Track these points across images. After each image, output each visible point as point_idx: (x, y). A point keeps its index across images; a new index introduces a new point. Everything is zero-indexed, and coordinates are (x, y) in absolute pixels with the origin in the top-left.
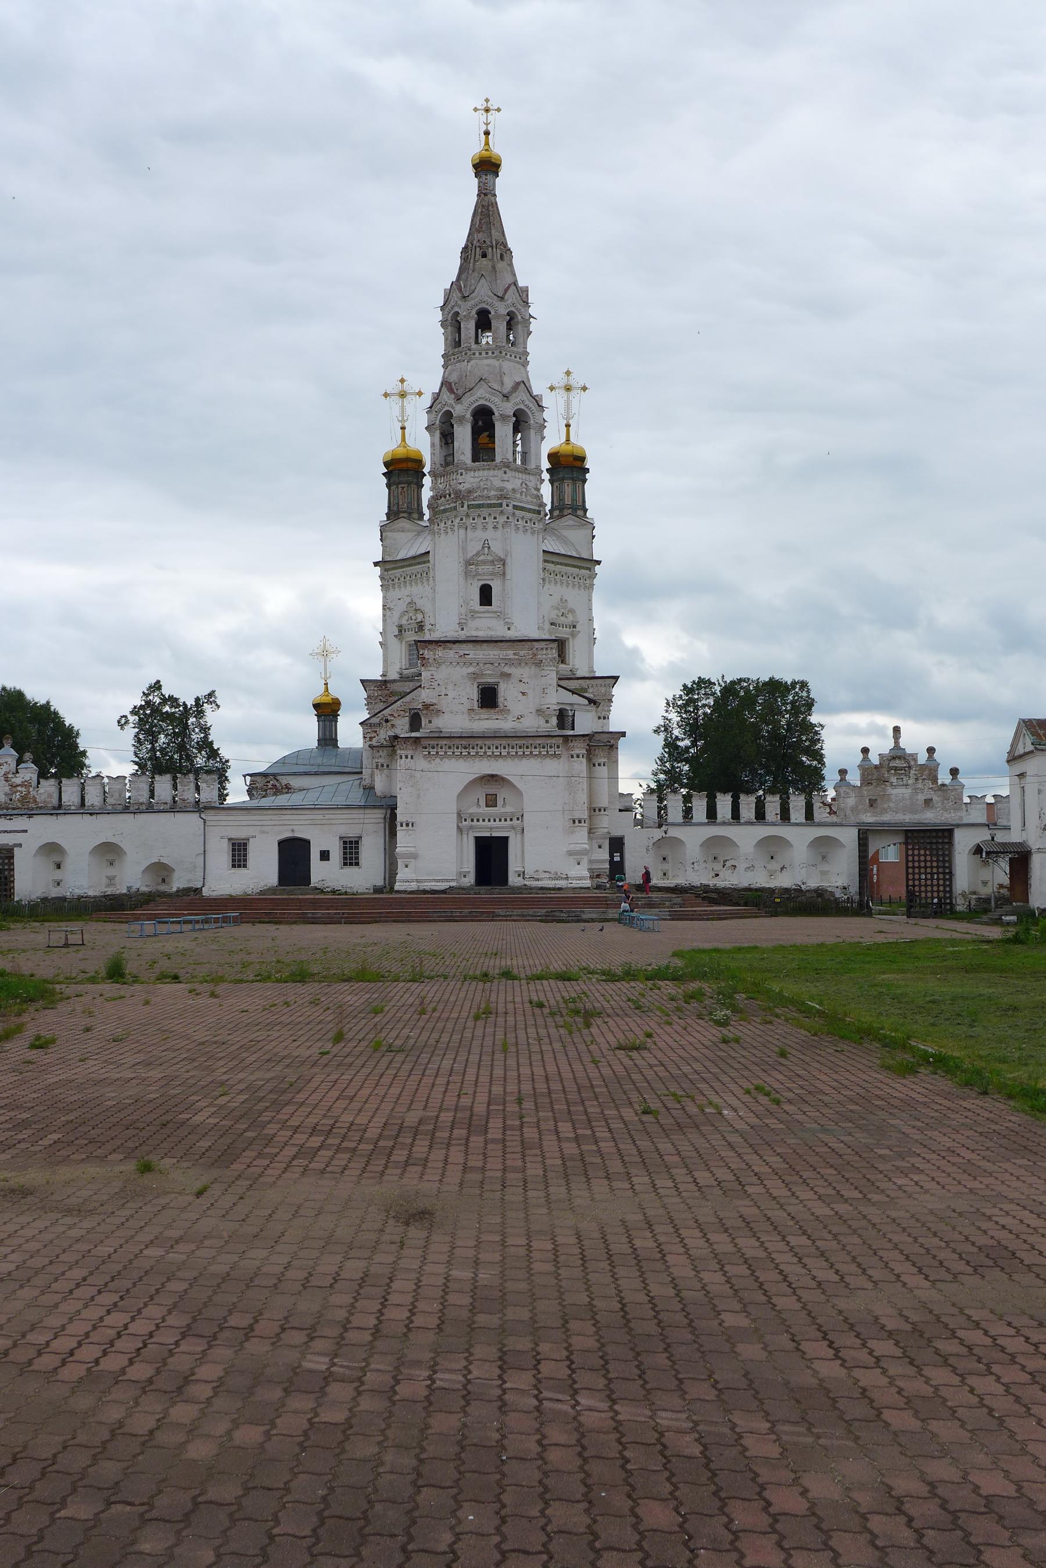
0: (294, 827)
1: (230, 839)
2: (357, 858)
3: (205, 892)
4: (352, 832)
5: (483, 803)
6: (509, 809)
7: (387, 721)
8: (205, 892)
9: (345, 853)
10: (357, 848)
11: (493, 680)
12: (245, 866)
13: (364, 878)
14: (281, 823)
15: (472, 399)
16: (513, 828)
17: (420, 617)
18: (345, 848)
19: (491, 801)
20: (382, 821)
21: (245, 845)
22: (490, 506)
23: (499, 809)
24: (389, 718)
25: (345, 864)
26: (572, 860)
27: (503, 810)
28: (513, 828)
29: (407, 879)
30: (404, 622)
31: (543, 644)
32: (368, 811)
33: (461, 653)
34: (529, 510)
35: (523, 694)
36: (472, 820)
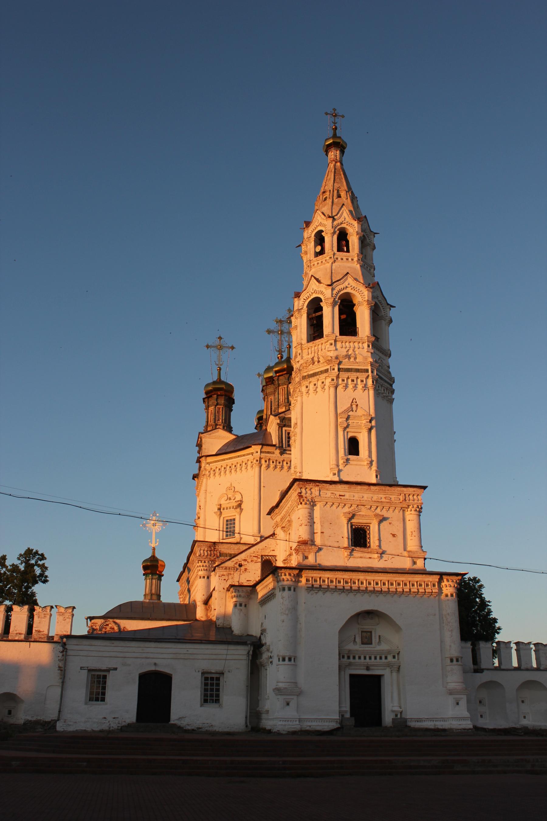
0: (157, 661)
1: (90, 671)
2: (218, 696)
3: (60, 727)
4: (214, 667)
5: (358, 640)
6: (384, 647)
7: (240, 565)
8: (60, 727)
9: (206, 690)
10: (218, 685)
11: (365, 521)
12: (103, 700)
13: (229, 715)
14: (144, 655)
15: (342, 286)
16: (389, 665)
17: (238, 498)
18: (206, 684)
19: (367, 639)
20: (245, 657)
21: (105, 677)
22: (357, 370)
23: (375, 647)
24: (243, 563)
25: (206, 701)
26: (451, 700)
27: (379, 648)
28: (389, 665)
29: (279, 717)
30: (223, 502)
31: (411, 490)
32: (232, 647)
33: (338, 493)
34: (386, 381)
35: (394, 535)
36: (349, 658)
